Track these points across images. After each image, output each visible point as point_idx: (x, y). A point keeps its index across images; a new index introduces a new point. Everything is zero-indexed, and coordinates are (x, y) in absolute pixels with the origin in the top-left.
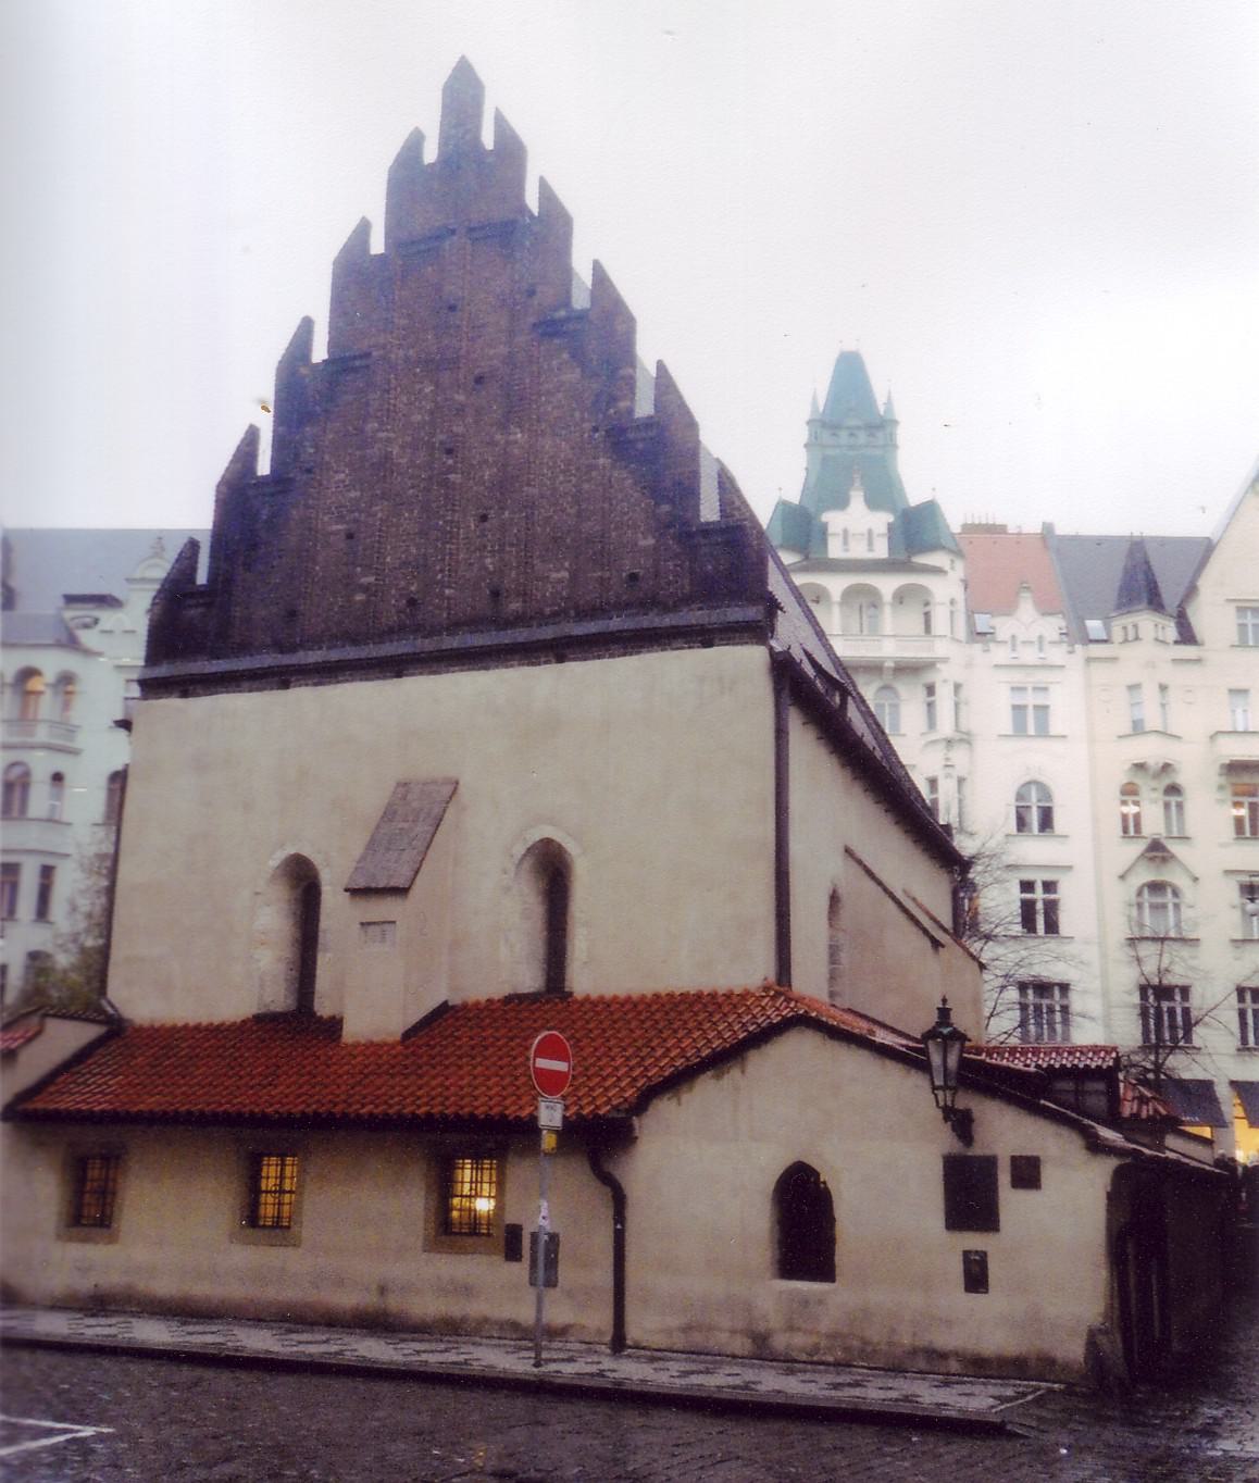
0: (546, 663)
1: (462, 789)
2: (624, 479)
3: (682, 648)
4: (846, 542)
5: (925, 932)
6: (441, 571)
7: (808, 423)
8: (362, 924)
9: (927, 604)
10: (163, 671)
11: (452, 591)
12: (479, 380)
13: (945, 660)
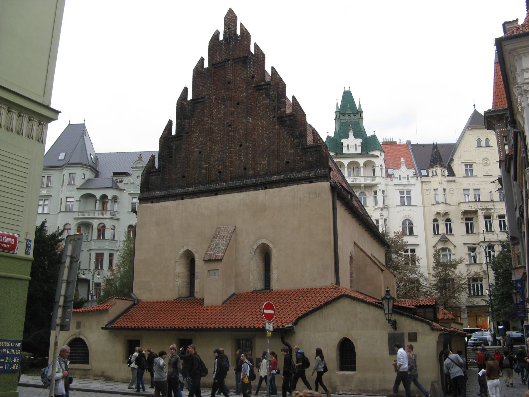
0: (261, 189)
1: (237, 229)
4: (348, 149)
5: (379, 267)
6: (228, 162)
7: (335, 112)
8: (209, 270)
9: (374, 166)
10: (145, 195)
13: (380, 183)
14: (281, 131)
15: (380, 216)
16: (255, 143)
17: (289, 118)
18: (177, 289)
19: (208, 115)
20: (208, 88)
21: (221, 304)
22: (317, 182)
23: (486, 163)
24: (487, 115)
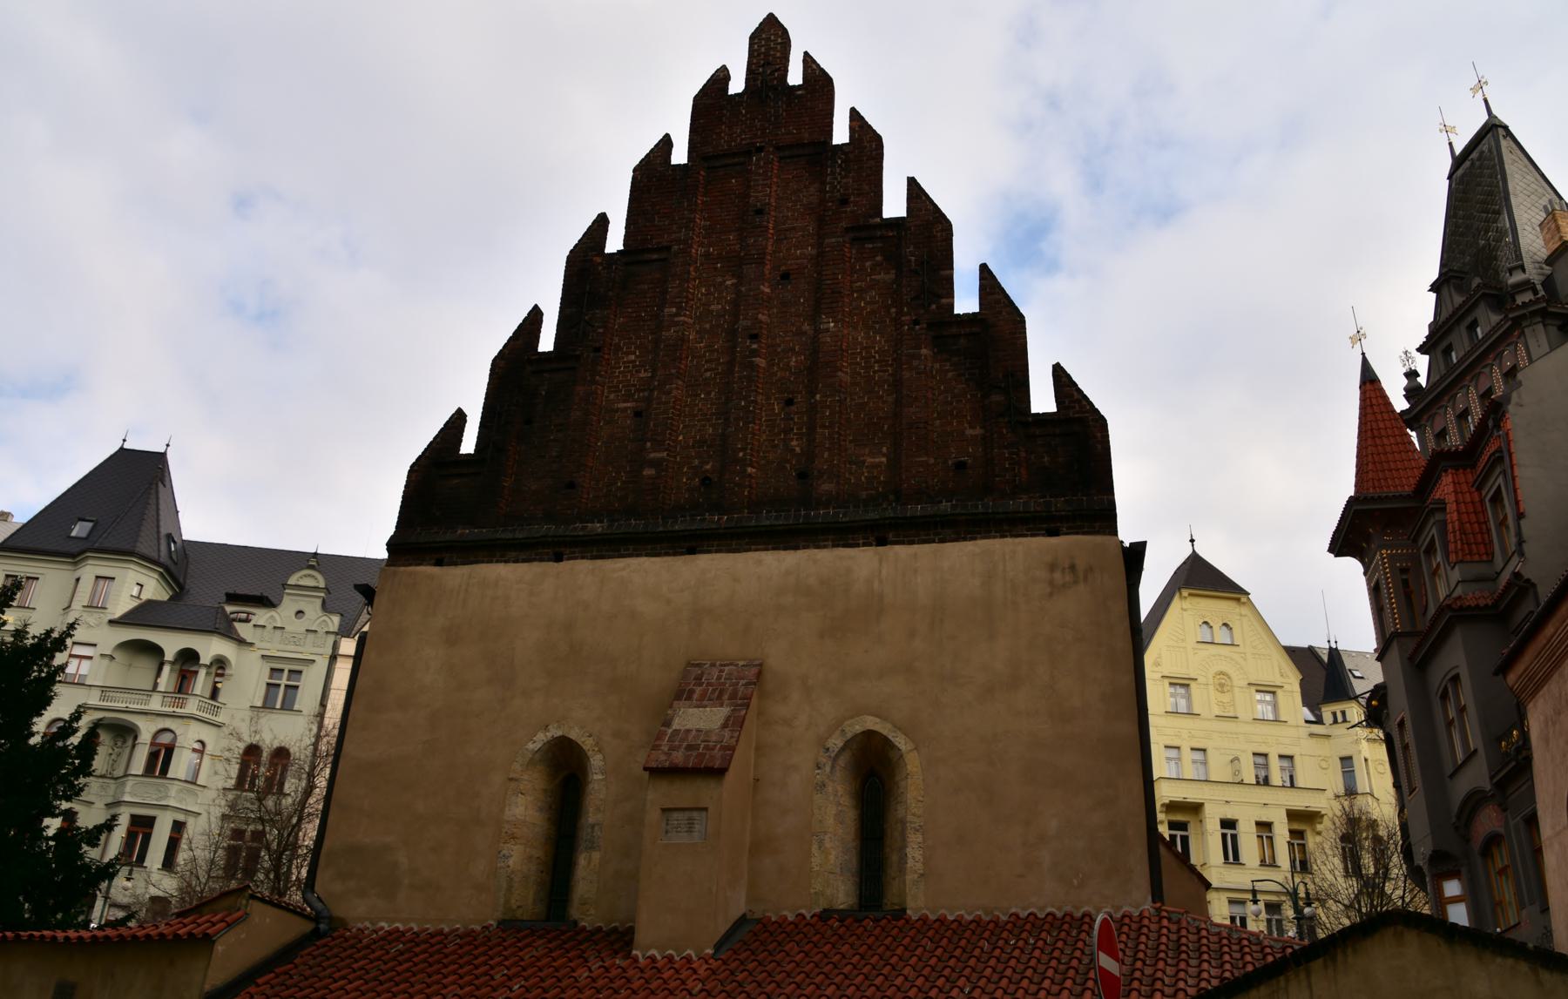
0: (865, 545)
2: (948, 371)
3: (1026, 536)
6: (741, 450)
8: (664, 810)
11: (754, 470)
12: (785, 276)
14: (937, 366)
16: (843, 396)
17: (968, 330)
18: (505, 885)
19: (677, 300)
20: (684, 221)
21: (710, 951)
22: (1077, 533)
23: (1222, 685)
24: (1355, 508)
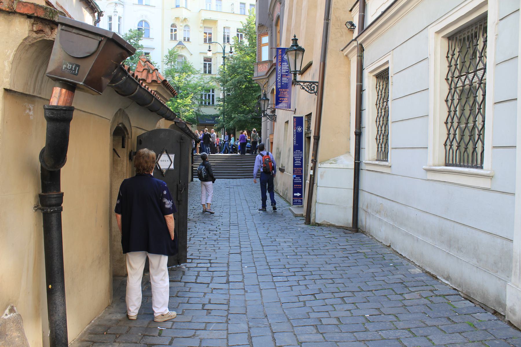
15: (114, 12)
